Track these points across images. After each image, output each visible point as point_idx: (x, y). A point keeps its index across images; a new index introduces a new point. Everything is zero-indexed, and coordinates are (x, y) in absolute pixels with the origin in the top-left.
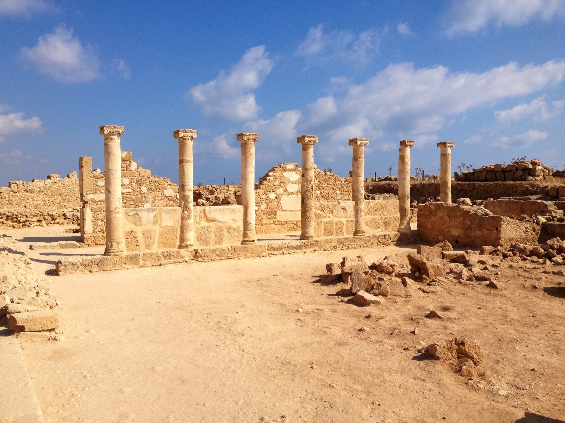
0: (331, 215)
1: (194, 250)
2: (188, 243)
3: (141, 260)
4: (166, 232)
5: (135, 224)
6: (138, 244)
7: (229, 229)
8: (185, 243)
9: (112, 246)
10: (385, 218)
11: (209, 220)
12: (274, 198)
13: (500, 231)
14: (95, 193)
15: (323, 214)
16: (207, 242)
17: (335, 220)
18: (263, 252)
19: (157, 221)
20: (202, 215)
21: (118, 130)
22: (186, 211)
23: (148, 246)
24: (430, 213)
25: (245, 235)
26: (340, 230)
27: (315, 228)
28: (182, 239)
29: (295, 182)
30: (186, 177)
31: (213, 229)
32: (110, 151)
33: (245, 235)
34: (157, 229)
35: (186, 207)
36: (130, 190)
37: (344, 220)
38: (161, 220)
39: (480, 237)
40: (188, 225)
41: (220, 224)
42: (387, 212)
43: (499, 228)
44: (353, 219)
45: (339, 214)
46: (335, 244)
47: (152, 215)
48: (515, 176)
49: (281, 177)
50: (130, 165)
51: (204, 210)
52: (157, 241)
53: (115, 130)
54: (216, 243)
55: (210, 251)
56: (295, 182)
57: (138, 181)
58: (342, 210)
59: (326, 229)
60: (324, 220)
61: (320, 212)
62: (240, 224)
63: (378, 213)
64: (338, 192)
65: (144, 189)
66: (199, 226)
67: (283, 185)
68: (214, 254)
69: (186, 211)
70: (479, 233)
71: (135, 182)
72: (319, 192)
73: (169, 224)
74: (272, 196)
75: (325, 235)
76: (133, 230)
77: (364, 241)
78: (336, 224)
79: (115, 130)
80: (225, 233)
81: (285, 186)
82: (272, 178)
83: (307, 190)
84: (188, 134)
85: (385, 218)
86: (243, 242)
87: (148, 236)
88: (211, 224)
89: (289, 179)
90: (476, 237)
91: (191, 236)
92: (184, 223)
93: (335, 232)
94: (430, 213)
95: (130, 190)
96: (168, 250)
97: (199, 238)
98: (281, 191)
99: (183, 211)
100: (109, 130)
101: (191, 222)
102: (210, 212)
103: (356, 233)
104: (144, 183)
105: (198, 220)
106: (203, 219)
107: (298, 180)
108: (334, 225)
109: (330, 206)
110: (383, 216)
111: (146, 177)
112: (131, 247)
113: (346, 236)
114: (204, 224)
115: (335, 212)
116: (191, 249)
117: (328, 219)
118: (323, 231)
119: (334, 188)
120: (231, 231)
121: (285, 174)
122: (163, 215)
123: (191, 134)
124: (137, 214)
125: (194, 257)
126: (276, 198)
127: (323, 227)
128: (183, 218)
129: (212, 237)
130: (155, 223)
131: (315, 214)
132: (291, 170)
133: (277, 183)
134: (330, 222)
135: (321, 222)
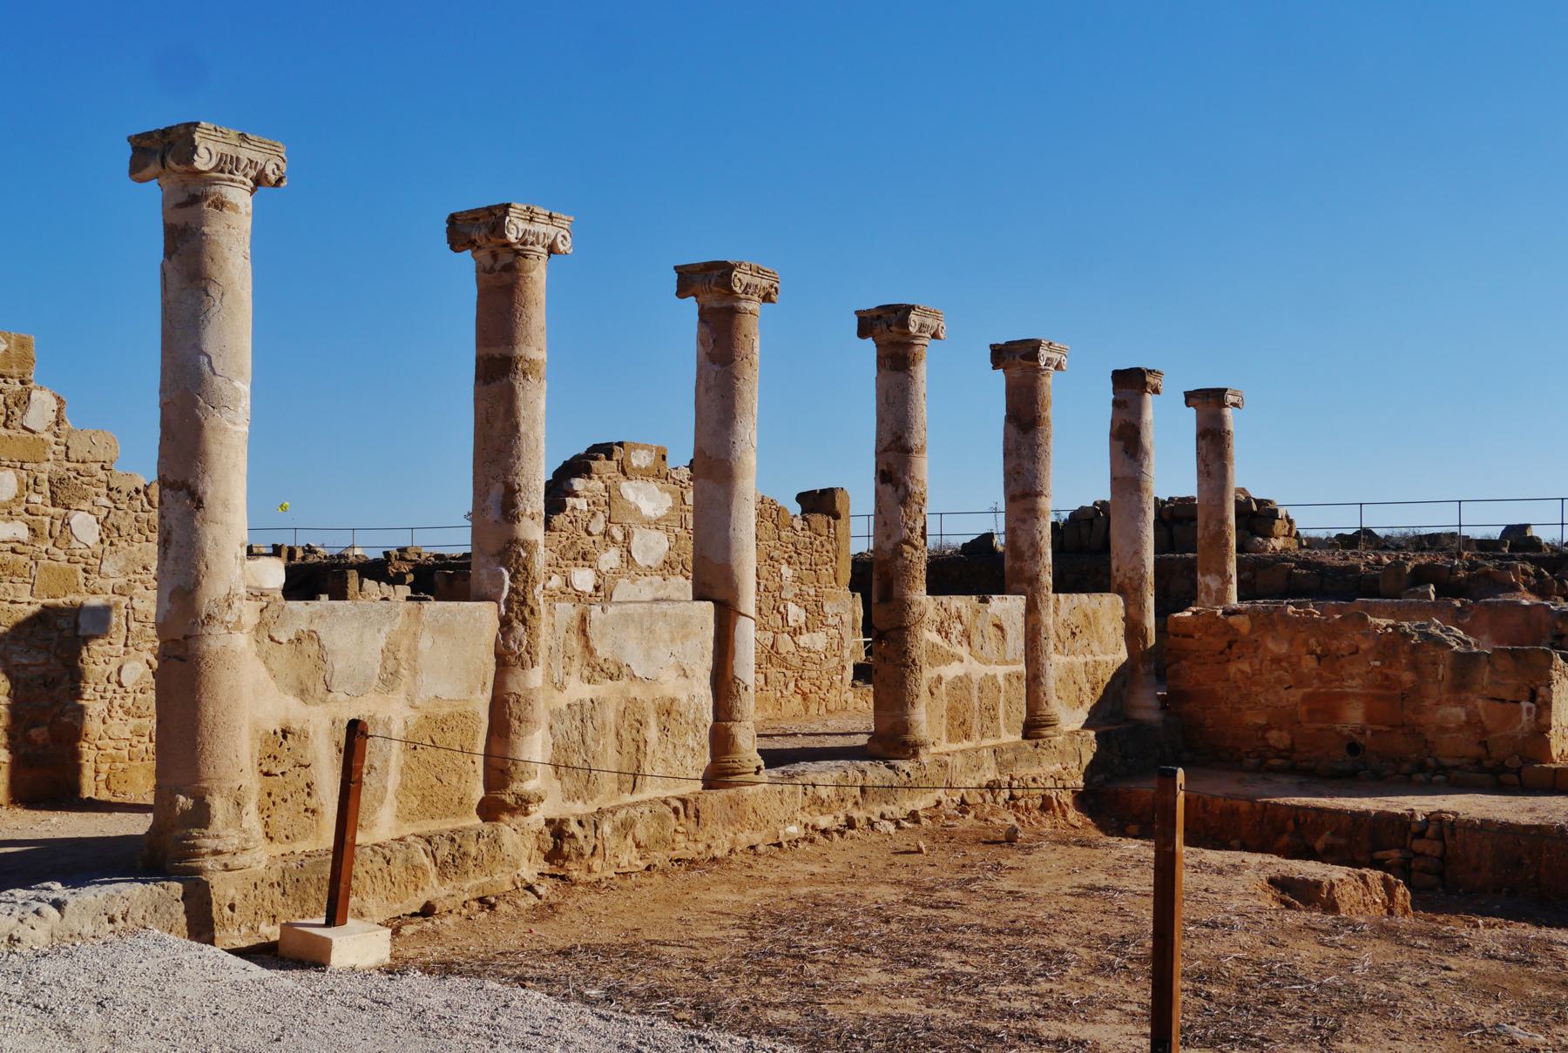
0: (963, 651)
1: (549, 822)
2: (530, 786)
5: (303, 693)
6: (312, 803)
7: (667, 710)
8: (514, 787)
9: (201, 816)
11: (598, 670)
12: (589, 589)
13: (1547, 705)
15: (945, 644)
17: (978, 670)
18: (791, 823)
19: (395, 674)
20: (575, 644)
21: (259, 157)
22: (520, 629)
24: (1230, 646)
28: (499, 771)
29: (655, 524)
30: (525, 446)
32: (212, 269)
35: (523, 603)
36: (23, 533)
38: (415, 672)
39: (1460, 728)
40: (525, 700)
41: (636, 691)
43: (1542, 690)
44: (1021, 668)
46: (990, 776)
49: (611, 499)
50: (24, 401)
51: (583, 619)
52: (393, 781)
53: (245, 154)
55: (615, 829)
56: (655, 524)
57: (57, 484)
58: (992, 630)
63: (1080, 642)
64: (785, 569)
65: (85, 527)
66: (561, 701)
67: (619, 536)
68: (630, 839)
69: (520, 629)
70: (1458, 713)
71: (45, 487)
76: (295, 726)
78: (981, 690)
79: (245, 154)
81: (627, 536)
82: (581, 504)
83: (908, 542)
84: (539, 228)
88: (603, 689)
89: (637, 509)
90: (1442, 729)
92: (513, 686)
93: (976, 724)
94: (1230, 646)
96: (448, 824)
98: (610, 559)
99: (505, 624)
100: (218, 149)
104: (85, 498)
105: (558, 673)
106: (577, 663)
107: (666, 518)
109: (964, 611)
110: (1089, 658)
111: (96, 467)
116: (538, 815)
118: (945, 721)
119: (775, 554)
120: (672, 725)
121: (632, 491)
122: (425, 643)
123: (551, 231)
124: (312, 635)
125: (549, 858)
126: (597, 588)
128: (506, 660)
129: (609, 758)
130: (389, 679)
132: (645, 474)
133: (598, 526)
134: (963, 682)
135: (940, 679)
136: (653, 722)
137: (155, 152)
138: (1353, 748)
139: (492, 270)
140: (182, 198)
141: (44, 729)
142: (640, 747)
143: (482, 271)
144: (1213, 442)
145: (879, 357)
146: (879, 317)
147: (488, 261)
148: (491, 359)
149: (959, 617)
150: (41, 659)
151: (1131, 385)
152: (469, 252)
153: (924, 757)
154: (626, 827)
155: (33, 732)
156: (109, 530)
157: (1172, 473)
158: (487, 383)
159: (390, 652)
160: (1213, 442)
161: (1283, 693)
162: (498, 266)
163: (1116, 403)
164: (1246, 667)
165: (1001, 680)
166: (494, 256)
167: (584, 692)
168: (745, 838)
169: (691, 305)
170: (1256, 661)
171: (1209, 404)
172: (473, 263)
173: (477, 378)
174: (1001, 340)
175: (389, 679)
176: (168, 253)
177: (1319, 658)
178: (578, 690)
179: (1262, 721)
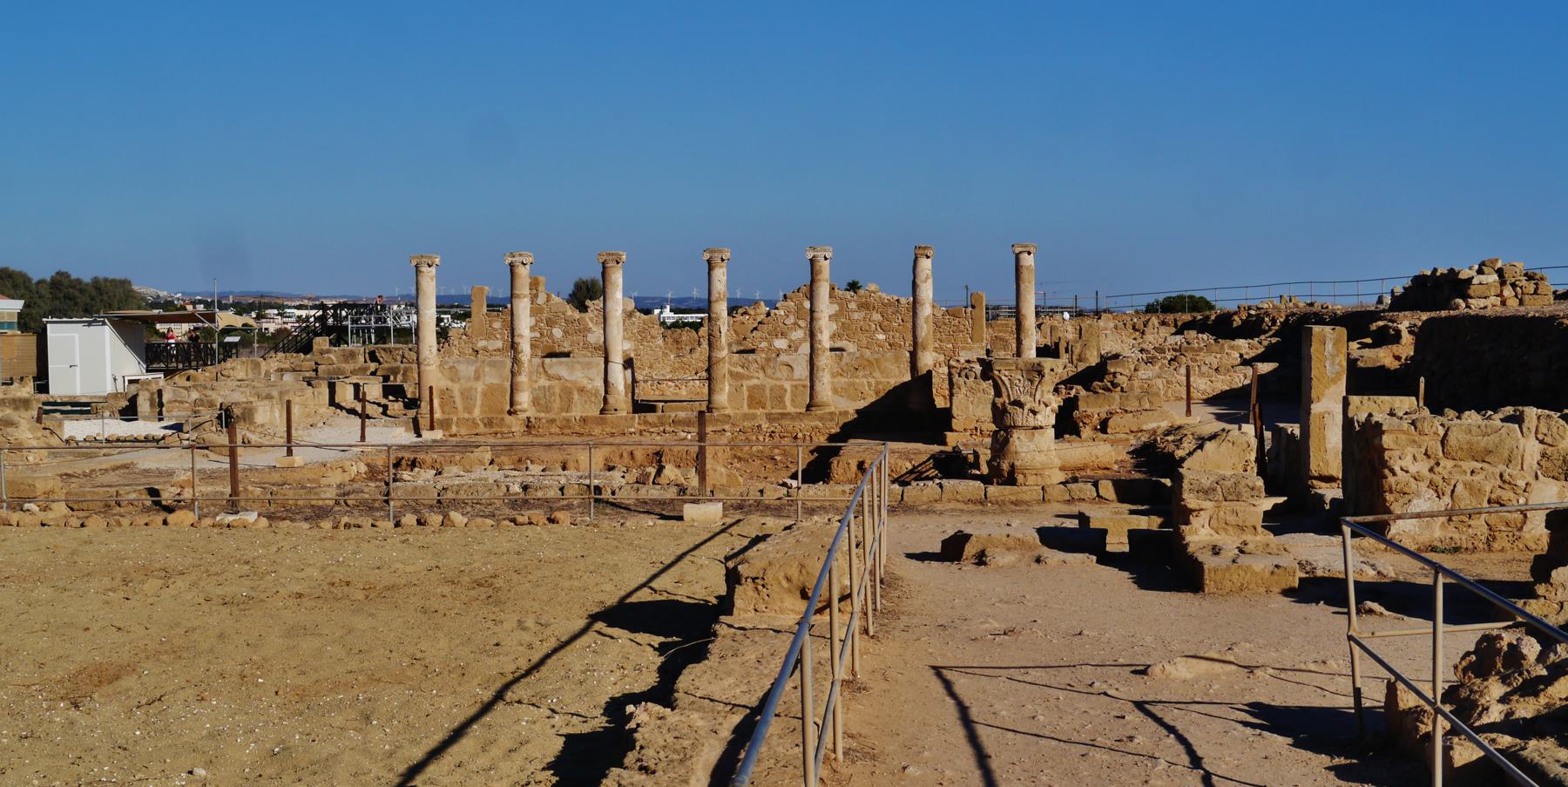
0: (761, 375)
4: (490, 392)
7: (582, 390)
10: (878, 383)
11: (549, 377)
14: (488, 339)
16: (547, 410)
17: (769, 383)
23: (469, 410)
25: (605, 400)
26: (779, 399)
27: (730, 394)
28: (512, 404)
31: (557, 390)
33: (605, 400)
34: (480, 387)
37: (787, 386)
42: (882, 372)
45: (778, 374)
47: (472, 369)
52: (479, 403)
54: (562, 410)
59: (751, 398)
60: (746, 383)
61: (740, 370)
62: (600, 384)
65: (557, 333)
72: (881, 337)
73: (495, 381)
74: (780, 343)
75: (750, 407)
77: (821, 419)
80: (576, 396)
85: (878, 383)
86: (602, 411)
87: (467, 395)
91: (524, 399)
93: (768, 403)
97: (535, 402)
101: (523, 379)
102: (551, 366)
103: (809, 407)
112: (447, 409)
113: (790, 409)
114: (543, 382)
115: (769, 371)
117: (755, 382)
127: (746, 394)
131: (731, 373)
133: (791, 320)
134: (761, 388)
142: (570, 400)
153: (716, 414)
156: (566, 332)
159: (476, 371)
167: (547, 383)
168: (608, 430)
175: (477, 378)
178: (543, 382)
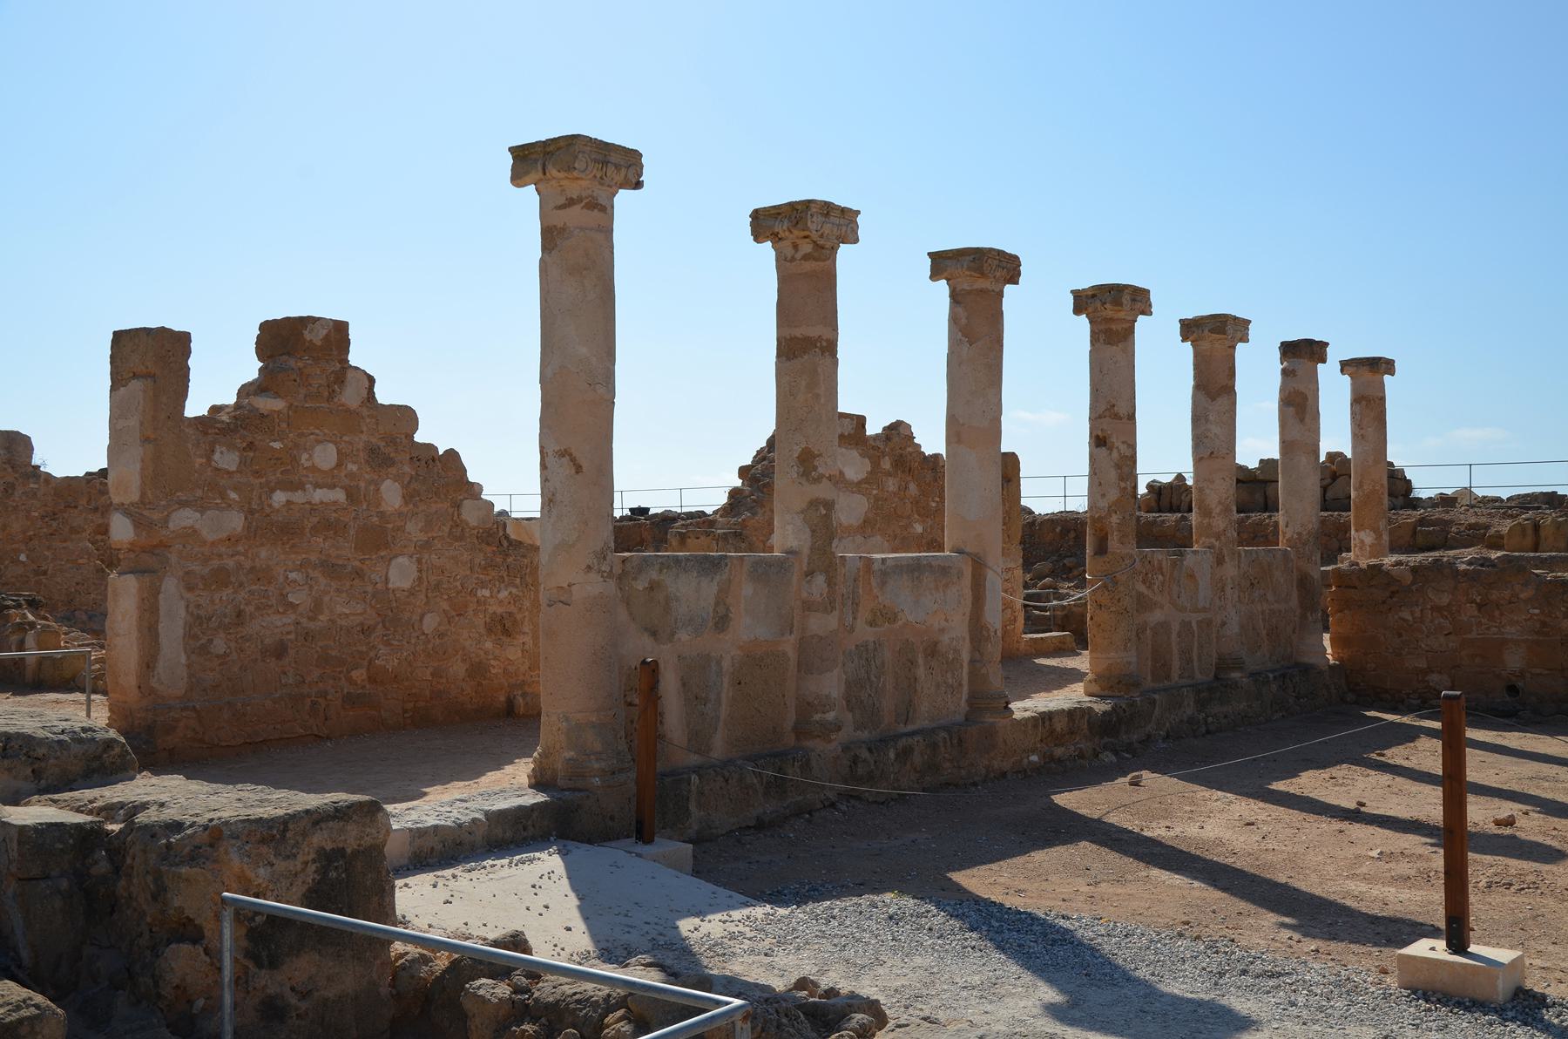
3: (692, 807)
46: (1189, 711)
48: (1329, 495)
55: (897, 755)
95: (339, 495)
108: (1174, 636)
134: (1164, 626)
136: (920, 661)
137: (536, 161)
138: (1512, 690)
139: (793, 259)
140: (562, 201)
141: (364, 671)
143: (781, 261)
144: (1369, 410)
145: (1092, 331)
146: (1094, 296)
147: (789, 252)
148: (793, 339)
149: (1161, 568)
150: (359, 608)
151: (1302, 355)
152: (769, 244)
154: (906, 753)
155: (355, 674)
157: (1335, 434)
158: (789, 359)
160: (1369, 410)
161: (1442, 639)
162: (798, 256)
163: (1284, 372)
164: (1406, 615)
165: (1194, 624)
166: (795, 246)
169: (942, 287)
170: (1417, 610)
171: (1370, 373)
172: (773, 253)
173: (778, 356)
174: (1190, 315)
176: (544, 248)
177: (1480, 607)
179: (1423, 664)
